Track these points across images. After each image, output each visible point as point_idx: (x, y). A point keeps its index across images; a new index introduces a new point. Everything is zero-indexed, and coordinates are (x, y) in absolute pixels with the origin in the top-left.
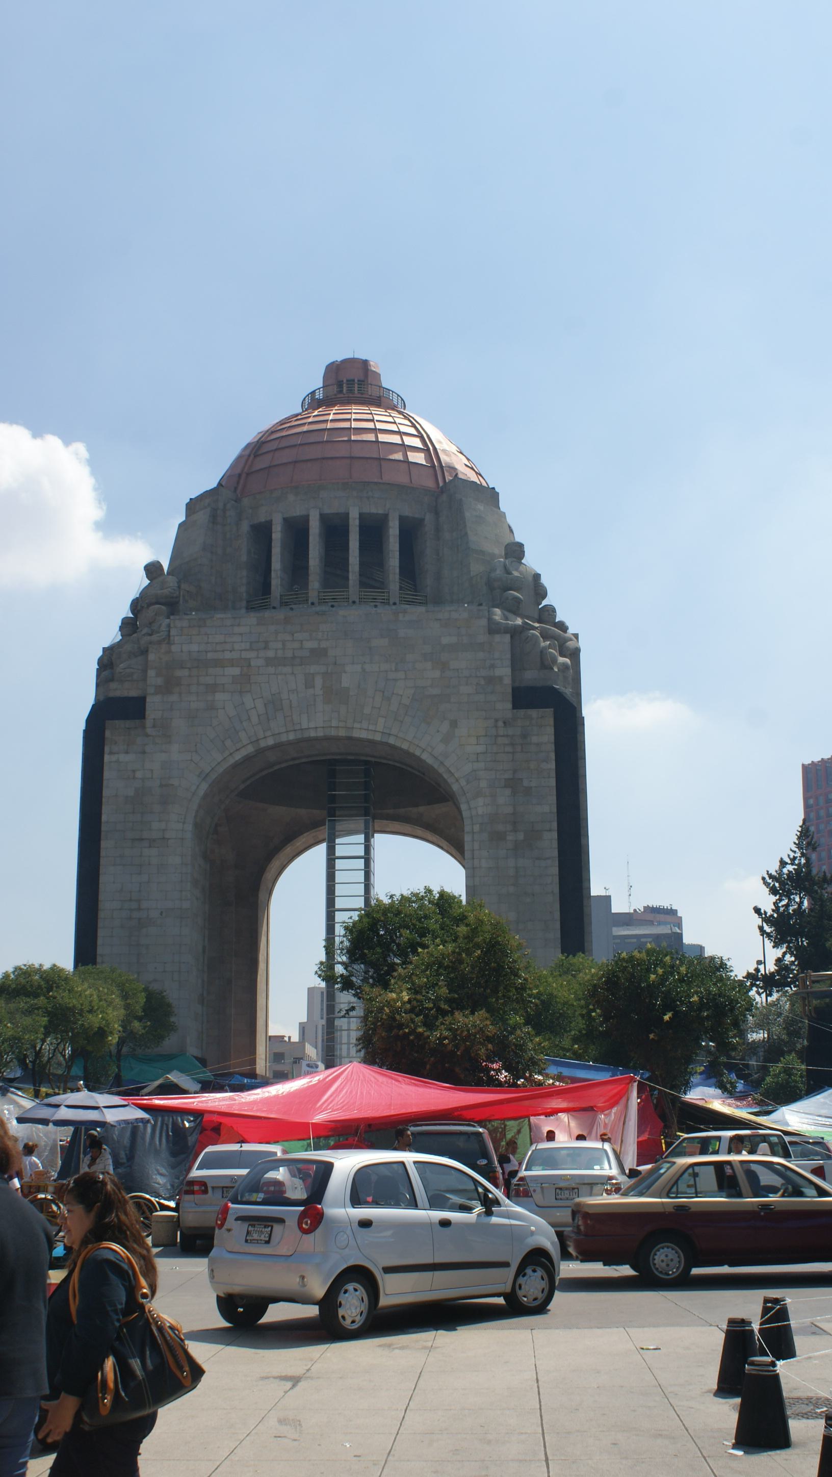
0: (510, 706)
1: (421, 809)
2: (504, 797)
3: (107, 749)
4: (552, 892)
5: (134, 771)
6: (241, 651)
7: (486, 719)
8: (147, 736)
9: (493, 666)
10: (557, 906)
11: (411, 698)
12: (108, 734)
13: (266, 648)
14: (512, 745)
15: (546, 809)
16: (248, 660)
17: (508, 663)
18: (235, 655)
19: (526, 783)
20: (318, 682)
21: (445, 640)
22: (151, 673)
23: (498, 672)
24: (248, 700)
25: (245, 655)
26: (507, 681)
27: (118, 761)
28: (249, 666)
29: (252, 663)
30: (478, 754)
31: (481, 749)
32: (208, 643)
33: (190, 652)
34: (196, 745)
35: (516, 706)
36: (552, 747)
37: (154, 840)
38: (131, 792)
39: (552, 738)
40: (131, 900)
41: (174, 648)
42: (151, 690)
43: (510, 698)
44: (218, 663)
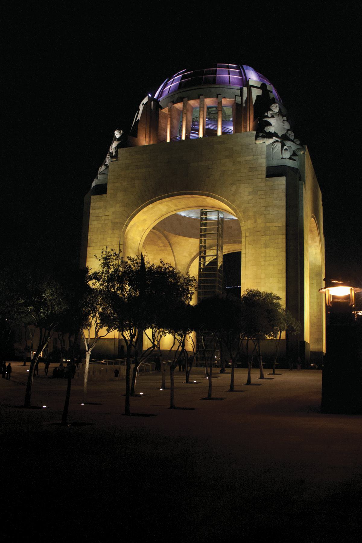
14: (265, 195)
15: (280, 224)
26: (264, 166)
38: (100, 226)
42: (109, 181)
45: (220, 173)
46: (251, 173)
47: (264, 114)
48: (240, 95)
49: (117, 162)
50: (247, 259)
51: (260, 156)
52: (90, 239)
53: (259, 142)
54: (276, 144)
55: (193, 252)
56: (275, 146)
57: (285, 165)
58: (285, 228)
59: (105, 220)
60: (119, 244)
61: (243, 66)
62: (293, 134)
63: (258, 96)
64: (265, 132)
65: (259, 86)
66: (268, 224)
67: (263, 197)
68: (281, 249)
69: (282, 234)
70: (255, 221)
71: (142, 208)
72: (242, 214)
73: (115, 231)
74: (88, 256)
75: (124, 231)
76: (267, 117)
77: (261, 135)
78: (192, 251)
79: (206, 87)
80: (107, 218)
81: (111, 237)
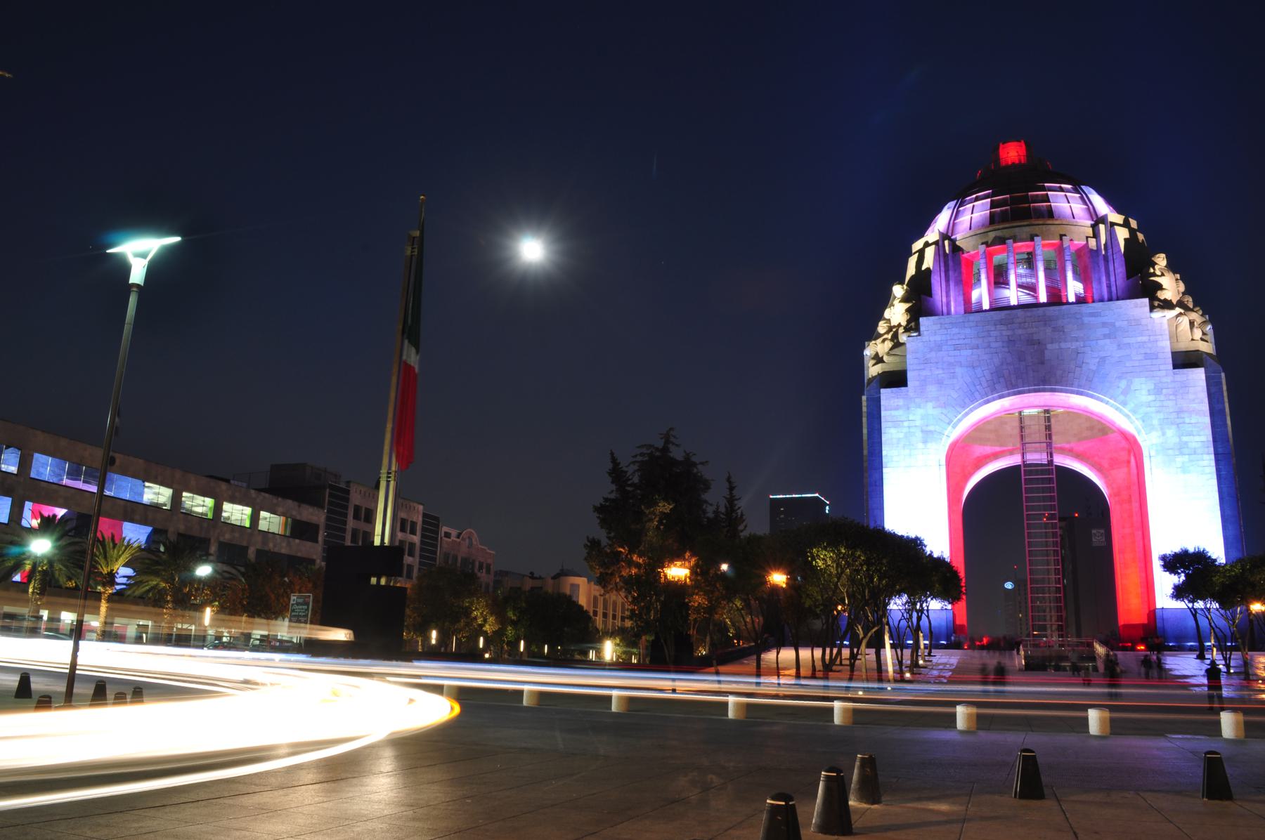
0: (1172, 367)
2: (1171, 432)
11: (1097, 364)
14: (1175, 394)
15: (1203, 438)
18: (966, 341)
22: (909, 356)
23: (1160, 344)
24: (979, 371)
32: (947, 334)
35: (1176, 366)
38: (901, 435)
42: (909, 368)
43: (1170, 361)
45: (1098, 360)
46: (1149, 362)
47: (1149, 269)
48: (1092, 236)
49: (919, 337)
51: (1160, 337)
52: (886, 455)
53: (1158, 315)
54: (1181, 319)
56: (1180, 321)
57: (1198, 351)
59: (909, 427)
61: (1082, 186)
62: (1191, 299)
63: (1125, 240)
64: (1159, 300)
65: (1121, 222)
66: (1185, 439)
67: (1171, 397)
68: (1210, 475)
69: (1208, 454)
70: (1164, 434)
72: (1141, 422)
73: (929, 445)
76: (1154, 275)
77: (1156, 303)
79: (1041, 222)
80: (912, 424)
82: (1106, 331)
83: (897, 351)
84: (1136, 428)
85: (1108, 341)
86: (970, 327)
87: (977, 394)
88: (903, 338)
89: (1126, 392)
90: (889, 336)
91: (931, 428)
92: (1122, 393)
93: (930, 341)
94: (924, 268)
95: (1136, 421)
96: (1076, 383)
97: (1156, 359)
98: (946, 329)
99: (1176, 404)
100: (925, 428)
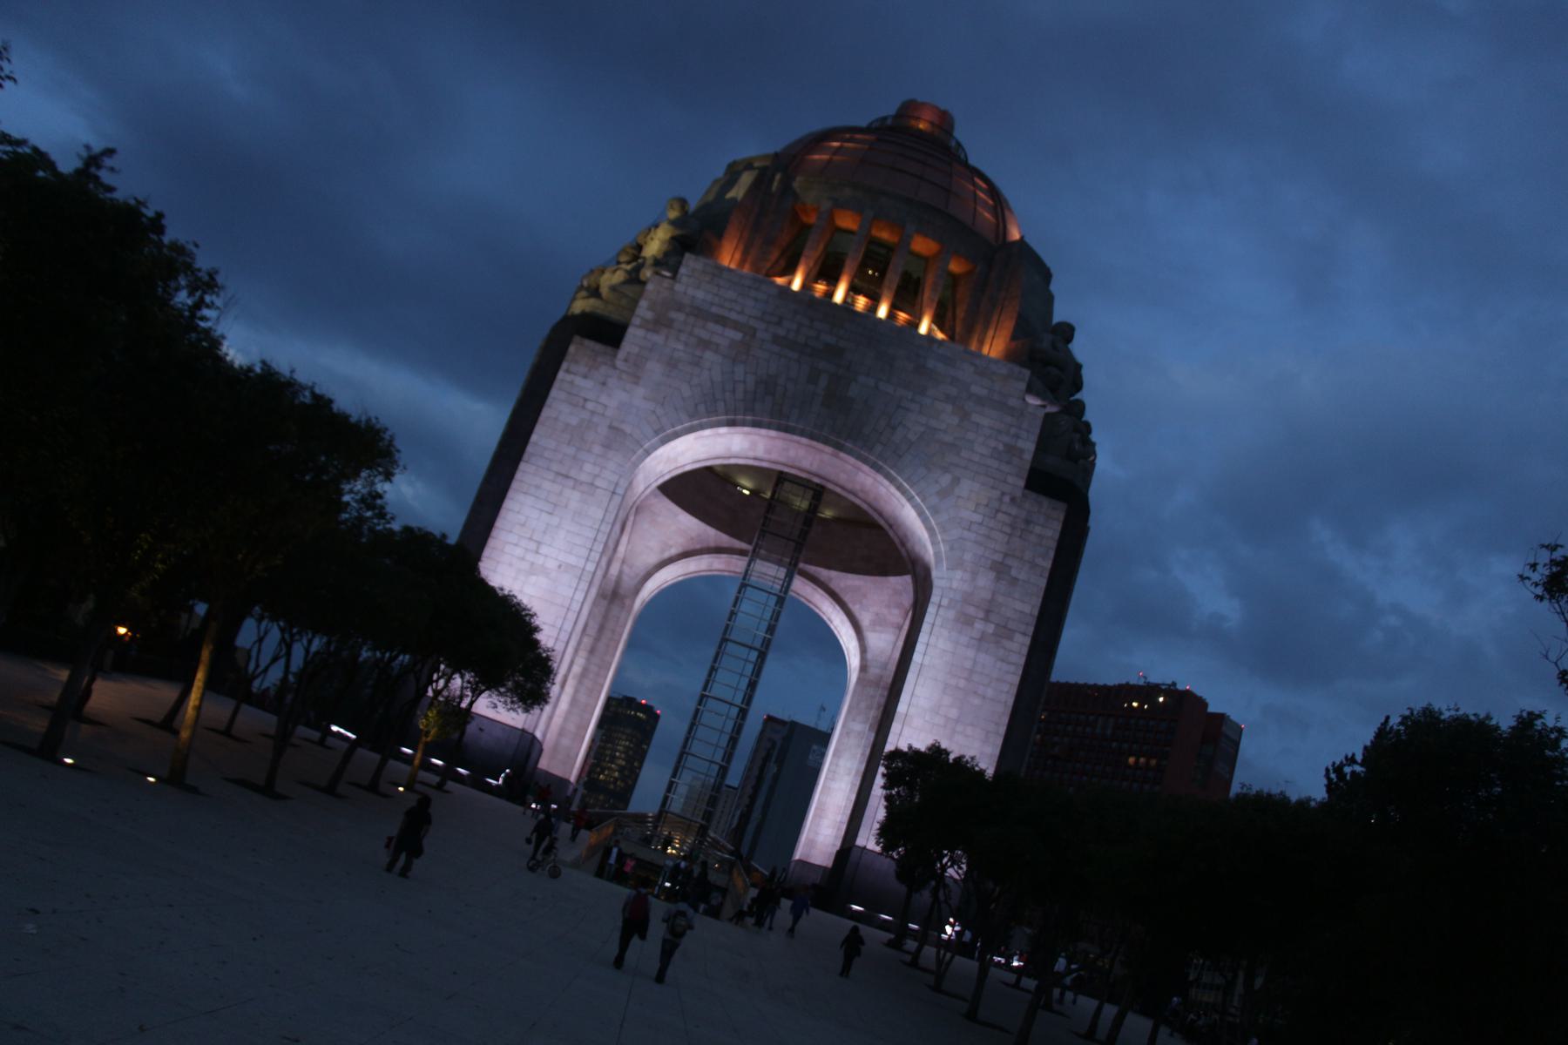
0: (1022, 483)
1: (833, 574)
2: (985, 581)
3: (564, 365)
4: (1006, 702)
5: (586, 400)
6: (750, 317)
7: (993, 488)
8: (614, 367)
9: (1017, 436)
10: (1005, 720)
12: (572, 349)
13: (779, 323)
14: (1013, 527)
15: (1027, 609)
16: (755, 330)
17: (1034, 438)
18: (742, 319)
19: (1014, 573)
20: (823, 382)
21: (975, 389)
22: (643, 304)
23: (1021, 444)
24: (740, 370)
25: (752, 323)
26: (1028, 457)
27: (572, 383)
28: (754, 336)
29: (759, 335)
30: (971, 522)
31: (977, 518)
32: (717, 295)
33: (693, 297)
34: (664, 398)
36: (1053, 545)
37: (582, 483)
38: (574, 421)
39: (1057, 536)
40: (530, 539)
41: (678, 287)
42: (636, 321)
43: (1025, 474)
44: (722, 321)
45: (922, 429)
46: (995, 464)
49: (671, 281)
50: (927, 658)
55: (671, 547)
58: (1033, 621)
59: (593, 413)
60: (612, 489)
66: (1000, 599)
67: (1008, 530)
68: (1012, 668)
69: (1024, 634)
71: (702, 427)
74: (515, 485)
75: (636, 465)
78: (671, 543)
81: (595, 464)
82: (953, 391)
83: (630, 290)
84: (937, 554)
85: (949, 408)
86: (756, 300)
87: (721, 405)
88: (647, 273)
89: (944, 494)
90: (629, 267)
91: (628, 429)
92: (938, 493)
93: (685, 293)
94: (730, 195)
95: (942, 545)
96: (879, 448)
97: (1008, 463)
98: (718, 285)
99: (1008, 543)
100: (615, 424)
